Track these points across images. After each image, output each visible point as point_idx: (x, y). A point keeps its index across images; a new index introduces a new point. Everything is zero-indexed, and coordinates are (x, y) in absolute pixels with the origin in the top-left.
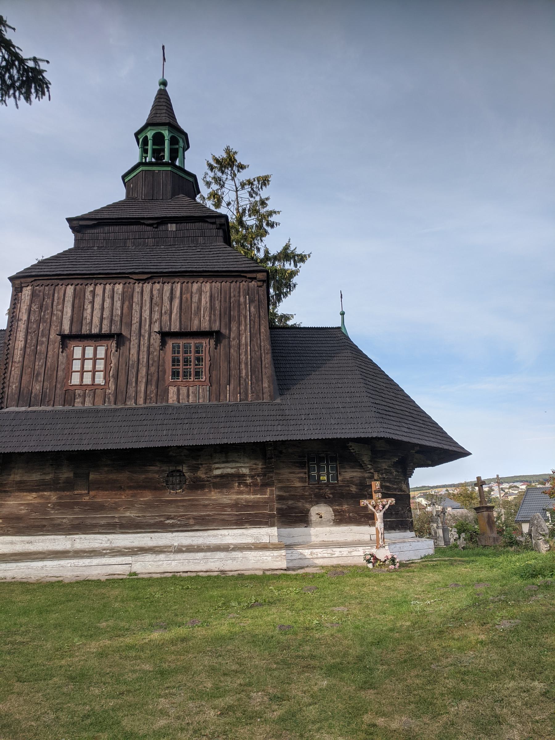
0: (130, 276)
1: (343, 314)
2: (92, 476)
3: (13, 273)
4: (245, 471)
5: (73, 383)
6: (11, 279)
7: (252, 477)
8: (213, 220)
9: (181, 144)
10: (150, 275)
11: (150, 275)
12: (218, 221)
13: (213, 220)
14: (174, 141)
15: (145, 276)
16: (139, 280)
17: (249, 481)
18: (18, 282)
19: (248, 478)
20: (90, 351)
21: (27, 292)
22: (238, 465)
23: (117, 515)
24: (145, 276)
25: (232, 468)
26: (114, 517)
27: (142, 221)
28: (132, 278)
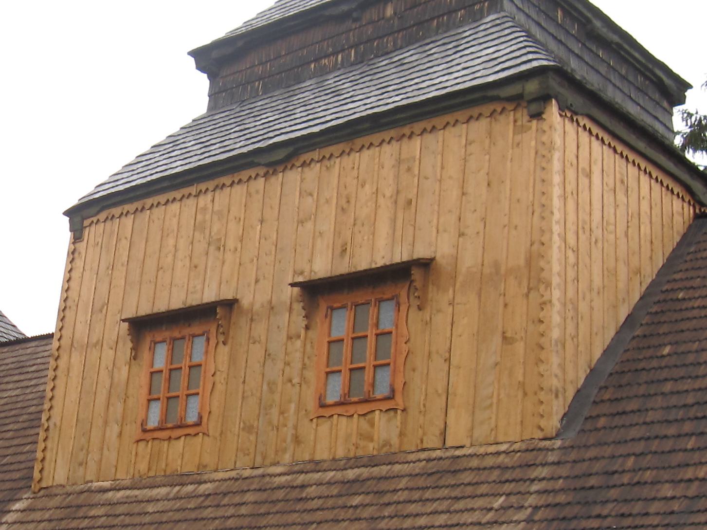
0: (256, 161)
3: (73, 202)
6: (67, 213)
10: (291, 149)
11: (291, 149)
15: (281, 154)
18: (77, 219)
21: (93, 233)
24: (281, 154)
28: (259, 165)
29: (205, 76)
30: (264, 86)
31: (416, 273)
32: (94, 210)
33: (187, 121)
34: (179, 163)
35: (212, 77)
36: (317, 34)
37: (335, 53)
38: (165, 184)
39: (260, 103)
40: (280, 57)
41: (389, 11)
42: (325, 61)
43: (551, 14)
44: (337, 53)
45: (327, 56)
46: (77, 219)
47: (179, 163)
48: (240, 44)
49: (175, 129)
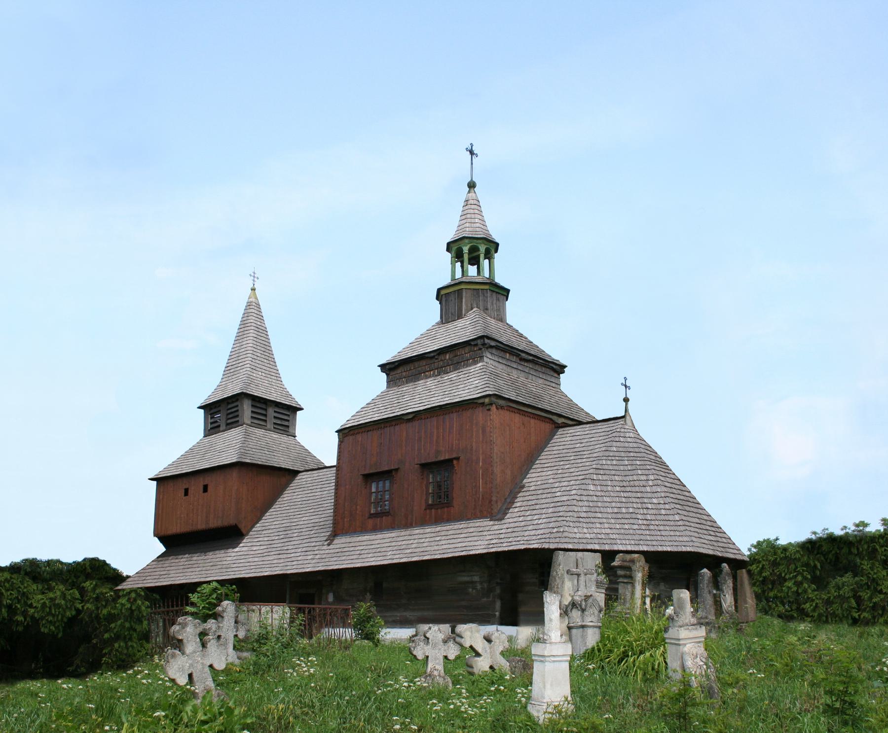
1: (626, 400)
2: (385, 585)
3: (338, 428)
4: (476, 579)
5: (372, 512)
6: (336, 432)
7: (481, 583)
8: (475, 342)
9: (482, 248)
10: (413, 415)
12: (479, 342)
13: (475, 342)
14: (474, 250)
16: (409, 420)
17: (479, 587)
18: (341, 434)
19: (478, 585)
20: (387, 483)
22: (472, 574)
23: (398, 614)
24: (410, 416)
25: (468, 576)
26: (397, 616)
27: (426, 356)
29: (385, 374)
30: (406, 381)
31: (455, 462)
32: (346, 431)
33: (379, 393)
34: (376, 415)
35: (388, 375)
36: (423, 363)
37: (430, 371)
38: (372, 423)
39: (405, 389)
40: (410, 370)
41: (447, 357)
42: (427, 373)
43: (503, 356)
44: (431, 371)
45: (427, 371)
46: (341, 434)
47: (376, 415)
48: (397, 364)
49: (374, 397)
